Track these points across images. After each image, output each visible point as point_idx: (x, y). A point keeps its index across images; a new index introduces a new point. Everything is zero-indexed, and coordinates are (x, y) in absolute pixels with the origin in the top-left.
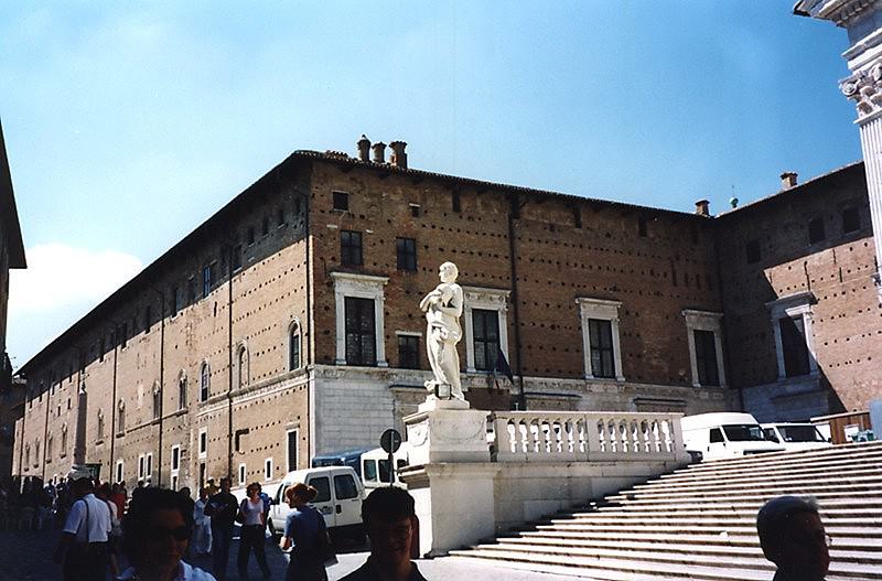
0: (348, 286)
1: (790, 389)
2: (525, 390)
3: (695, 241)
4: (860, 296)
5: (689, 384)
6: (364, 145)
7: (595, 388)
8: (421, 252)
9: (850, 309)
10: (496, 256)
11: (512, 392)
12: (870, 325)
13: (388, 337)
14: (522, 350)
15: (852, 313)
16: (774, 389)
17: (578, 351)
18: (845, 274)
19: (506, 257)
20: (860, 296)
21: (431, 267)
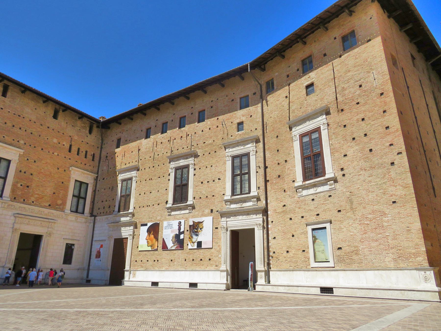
3: (90, 132)
4: (161, 169)
5: (63, 210)
9: (155, 176)
12: (162, 185)
15: (156, 178)
18: (156, 156)
20: (161, 169)
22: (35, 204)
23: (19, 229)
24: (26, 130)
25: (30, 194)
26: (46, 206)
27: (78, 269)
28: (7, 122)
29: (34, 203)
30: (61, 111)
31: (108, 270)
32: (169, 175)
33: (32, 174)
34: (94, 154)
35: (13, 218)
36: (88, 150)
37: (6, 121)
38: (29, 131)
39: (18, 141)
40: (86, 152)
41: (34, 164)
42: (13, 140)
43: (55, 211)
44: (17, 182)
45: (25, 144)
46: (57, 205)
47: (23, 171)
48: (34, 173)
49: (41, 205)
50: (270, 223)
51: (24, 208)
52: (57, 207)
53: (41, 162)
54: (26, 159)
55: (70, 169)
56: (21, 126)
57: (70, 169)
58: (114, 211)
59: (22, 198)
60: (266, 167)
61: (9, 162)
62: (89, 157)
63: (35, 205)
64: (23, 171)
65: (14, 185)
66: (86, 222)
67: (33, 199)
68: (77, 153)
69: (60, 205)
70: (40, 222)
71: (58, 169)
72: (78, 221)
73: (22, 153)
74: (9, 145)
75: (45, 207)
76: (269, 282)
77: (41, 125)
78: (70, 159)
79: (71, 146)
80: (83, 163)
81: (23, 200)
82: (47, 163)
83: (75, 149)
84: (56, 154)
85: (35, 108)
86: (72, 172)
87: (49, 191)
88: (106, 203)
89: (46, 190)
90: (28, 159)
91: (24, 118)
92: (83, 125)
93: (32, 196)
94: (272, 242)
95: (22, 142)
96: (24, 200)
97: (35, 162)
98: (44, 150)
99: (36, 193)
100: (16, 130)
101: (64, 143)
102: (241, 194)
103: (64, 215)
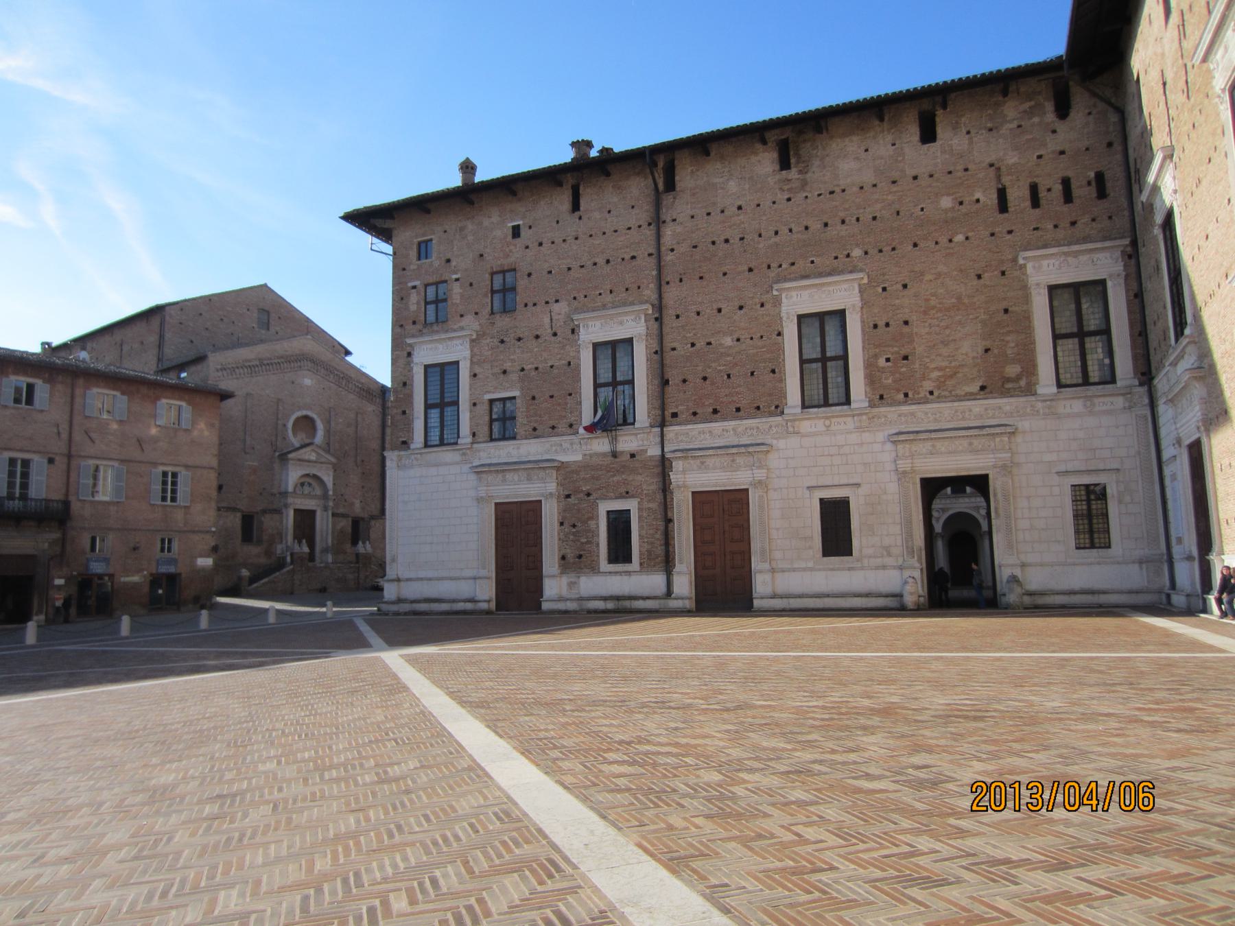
0: (429, 352)
2: (666, 450)
3: (1063, 110)
6: (468, 168)
7: (805, 426)
8: (522, 283)
10: (633, 257)
11: (650, 453)
13: (475, 404)
14: (670, 390)
17: (773, 371)
19: (650, 255)
21: (535, 300)
22: (938, 397)
23: (913, 471)
24: (858, 219)
25: (918, 375)
26: (972, 394)
27: (1141, 562)
28: (809, 224)
29: (936, 394)
30: (939, 112)
33: (906, 323)
34: (1100, 177)
35: (889, 446)
36: (1070, 173)
37: (805, 223)
38: (866, 217)
39: (848, 256)
40: (1066, 183)
41: (906, 292)
42: (836, 258)
43: (1005, 400)
44: (876, 356)
45: (866, 253)
46: (1009, 380)
47: (881, 323)
48: (913, 318)
49: (957, 396)
51: (913, 414)
52: (1009, 385)
53: (921, 281)
54: (880, 290)
55: (1021, 262)
56: (842, 214)
57: (1021, 262)
59: (898, 391)
61: (841, 314)
62: (1082, 191)
63: (940, 399)
64: (881, 323)
65: (870, 366)
66: (1130, 408)
67: (928, 385)
68: (1028, 203)
69: (1018, 378)
70: (965, 443)
71: (979, 277)
72: (1097, 408)
73: (865, 281)
74: (830, 274)
75: (970, 396)
77: (894, 182)
78: (1010, 232)
79: (1002, 194)
80: (1065, 223)
81: (902, 396)
82: (939, 275)
83: (1018, 195)
84: (959, 238)
85: (863, 148)
86: (1029, 266)
87: (968, 348)
89: (957, 349)
90: (884, 289)
91: (844, 191)
92: (1027, 105)
93: (924, 378)
95: (857, 253)
96: (906, 395)
97: (905, 286)
98: (922, 244)
99: (933, 366)
100: (832, 232)
101: (978, 195)
103: (1040, 405)
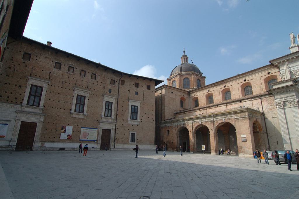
1: (27, 109)
16: (18, 108)
31: (15, 141)
32: (73, 96)
50: (116, 129)
58: (21, 103)
60: (117, 110)
76: (114, 147)
88: (12, 94)
94: (116, 135)
102: (108, 116)
